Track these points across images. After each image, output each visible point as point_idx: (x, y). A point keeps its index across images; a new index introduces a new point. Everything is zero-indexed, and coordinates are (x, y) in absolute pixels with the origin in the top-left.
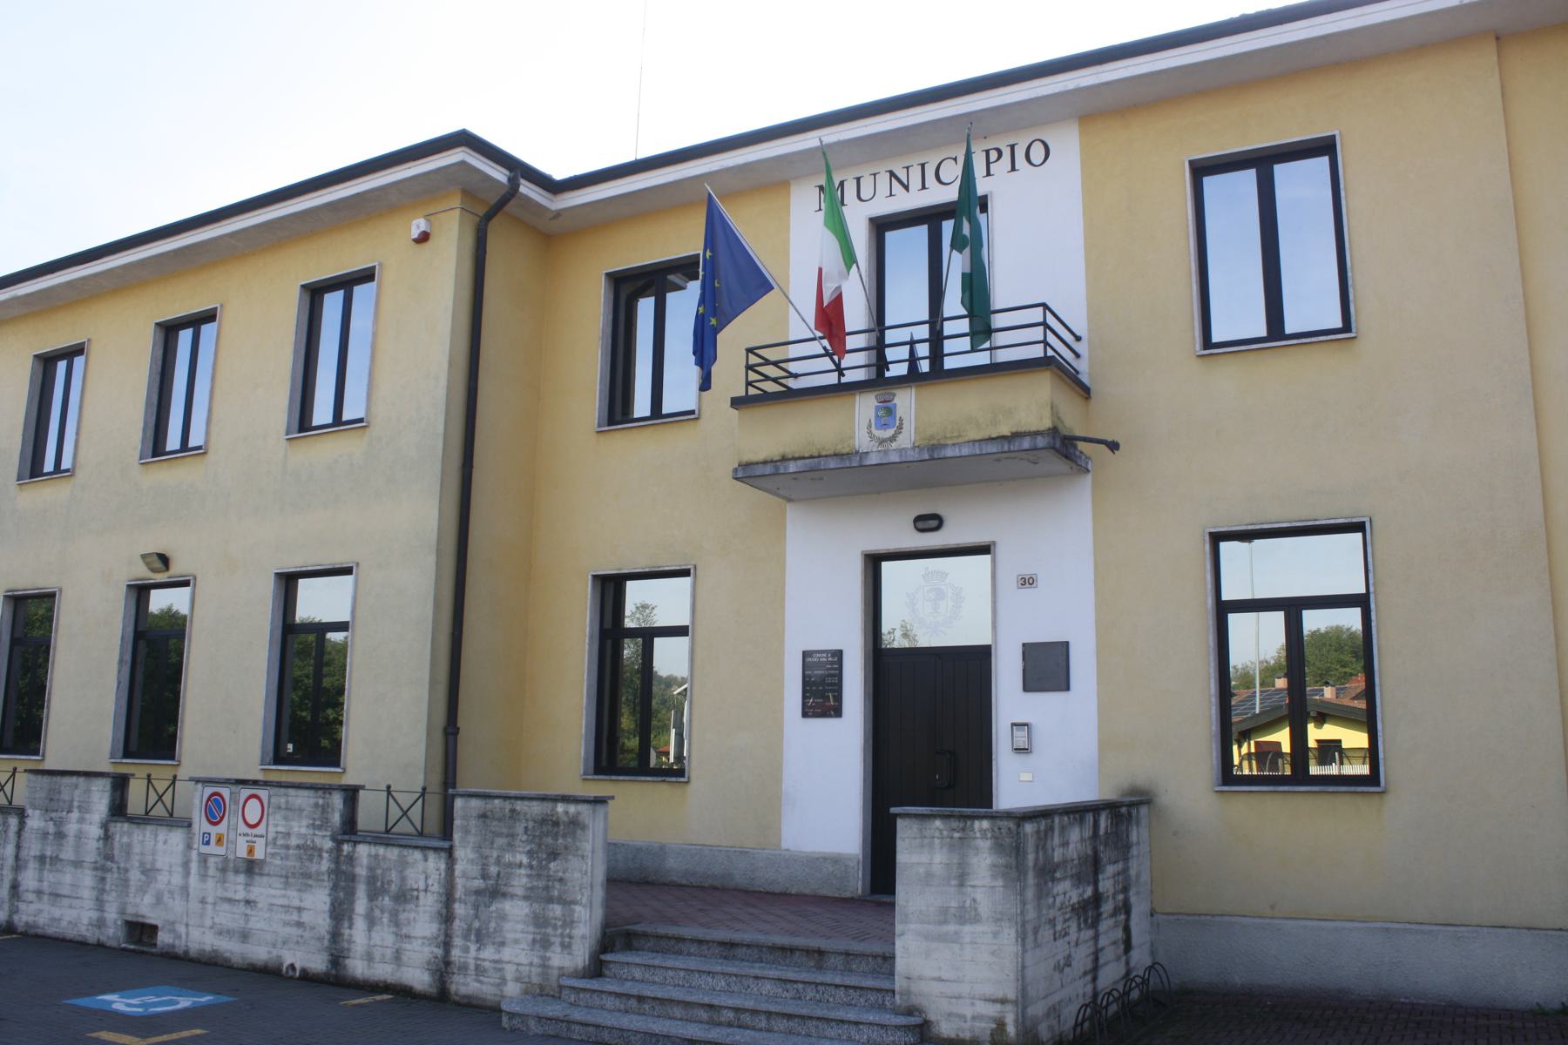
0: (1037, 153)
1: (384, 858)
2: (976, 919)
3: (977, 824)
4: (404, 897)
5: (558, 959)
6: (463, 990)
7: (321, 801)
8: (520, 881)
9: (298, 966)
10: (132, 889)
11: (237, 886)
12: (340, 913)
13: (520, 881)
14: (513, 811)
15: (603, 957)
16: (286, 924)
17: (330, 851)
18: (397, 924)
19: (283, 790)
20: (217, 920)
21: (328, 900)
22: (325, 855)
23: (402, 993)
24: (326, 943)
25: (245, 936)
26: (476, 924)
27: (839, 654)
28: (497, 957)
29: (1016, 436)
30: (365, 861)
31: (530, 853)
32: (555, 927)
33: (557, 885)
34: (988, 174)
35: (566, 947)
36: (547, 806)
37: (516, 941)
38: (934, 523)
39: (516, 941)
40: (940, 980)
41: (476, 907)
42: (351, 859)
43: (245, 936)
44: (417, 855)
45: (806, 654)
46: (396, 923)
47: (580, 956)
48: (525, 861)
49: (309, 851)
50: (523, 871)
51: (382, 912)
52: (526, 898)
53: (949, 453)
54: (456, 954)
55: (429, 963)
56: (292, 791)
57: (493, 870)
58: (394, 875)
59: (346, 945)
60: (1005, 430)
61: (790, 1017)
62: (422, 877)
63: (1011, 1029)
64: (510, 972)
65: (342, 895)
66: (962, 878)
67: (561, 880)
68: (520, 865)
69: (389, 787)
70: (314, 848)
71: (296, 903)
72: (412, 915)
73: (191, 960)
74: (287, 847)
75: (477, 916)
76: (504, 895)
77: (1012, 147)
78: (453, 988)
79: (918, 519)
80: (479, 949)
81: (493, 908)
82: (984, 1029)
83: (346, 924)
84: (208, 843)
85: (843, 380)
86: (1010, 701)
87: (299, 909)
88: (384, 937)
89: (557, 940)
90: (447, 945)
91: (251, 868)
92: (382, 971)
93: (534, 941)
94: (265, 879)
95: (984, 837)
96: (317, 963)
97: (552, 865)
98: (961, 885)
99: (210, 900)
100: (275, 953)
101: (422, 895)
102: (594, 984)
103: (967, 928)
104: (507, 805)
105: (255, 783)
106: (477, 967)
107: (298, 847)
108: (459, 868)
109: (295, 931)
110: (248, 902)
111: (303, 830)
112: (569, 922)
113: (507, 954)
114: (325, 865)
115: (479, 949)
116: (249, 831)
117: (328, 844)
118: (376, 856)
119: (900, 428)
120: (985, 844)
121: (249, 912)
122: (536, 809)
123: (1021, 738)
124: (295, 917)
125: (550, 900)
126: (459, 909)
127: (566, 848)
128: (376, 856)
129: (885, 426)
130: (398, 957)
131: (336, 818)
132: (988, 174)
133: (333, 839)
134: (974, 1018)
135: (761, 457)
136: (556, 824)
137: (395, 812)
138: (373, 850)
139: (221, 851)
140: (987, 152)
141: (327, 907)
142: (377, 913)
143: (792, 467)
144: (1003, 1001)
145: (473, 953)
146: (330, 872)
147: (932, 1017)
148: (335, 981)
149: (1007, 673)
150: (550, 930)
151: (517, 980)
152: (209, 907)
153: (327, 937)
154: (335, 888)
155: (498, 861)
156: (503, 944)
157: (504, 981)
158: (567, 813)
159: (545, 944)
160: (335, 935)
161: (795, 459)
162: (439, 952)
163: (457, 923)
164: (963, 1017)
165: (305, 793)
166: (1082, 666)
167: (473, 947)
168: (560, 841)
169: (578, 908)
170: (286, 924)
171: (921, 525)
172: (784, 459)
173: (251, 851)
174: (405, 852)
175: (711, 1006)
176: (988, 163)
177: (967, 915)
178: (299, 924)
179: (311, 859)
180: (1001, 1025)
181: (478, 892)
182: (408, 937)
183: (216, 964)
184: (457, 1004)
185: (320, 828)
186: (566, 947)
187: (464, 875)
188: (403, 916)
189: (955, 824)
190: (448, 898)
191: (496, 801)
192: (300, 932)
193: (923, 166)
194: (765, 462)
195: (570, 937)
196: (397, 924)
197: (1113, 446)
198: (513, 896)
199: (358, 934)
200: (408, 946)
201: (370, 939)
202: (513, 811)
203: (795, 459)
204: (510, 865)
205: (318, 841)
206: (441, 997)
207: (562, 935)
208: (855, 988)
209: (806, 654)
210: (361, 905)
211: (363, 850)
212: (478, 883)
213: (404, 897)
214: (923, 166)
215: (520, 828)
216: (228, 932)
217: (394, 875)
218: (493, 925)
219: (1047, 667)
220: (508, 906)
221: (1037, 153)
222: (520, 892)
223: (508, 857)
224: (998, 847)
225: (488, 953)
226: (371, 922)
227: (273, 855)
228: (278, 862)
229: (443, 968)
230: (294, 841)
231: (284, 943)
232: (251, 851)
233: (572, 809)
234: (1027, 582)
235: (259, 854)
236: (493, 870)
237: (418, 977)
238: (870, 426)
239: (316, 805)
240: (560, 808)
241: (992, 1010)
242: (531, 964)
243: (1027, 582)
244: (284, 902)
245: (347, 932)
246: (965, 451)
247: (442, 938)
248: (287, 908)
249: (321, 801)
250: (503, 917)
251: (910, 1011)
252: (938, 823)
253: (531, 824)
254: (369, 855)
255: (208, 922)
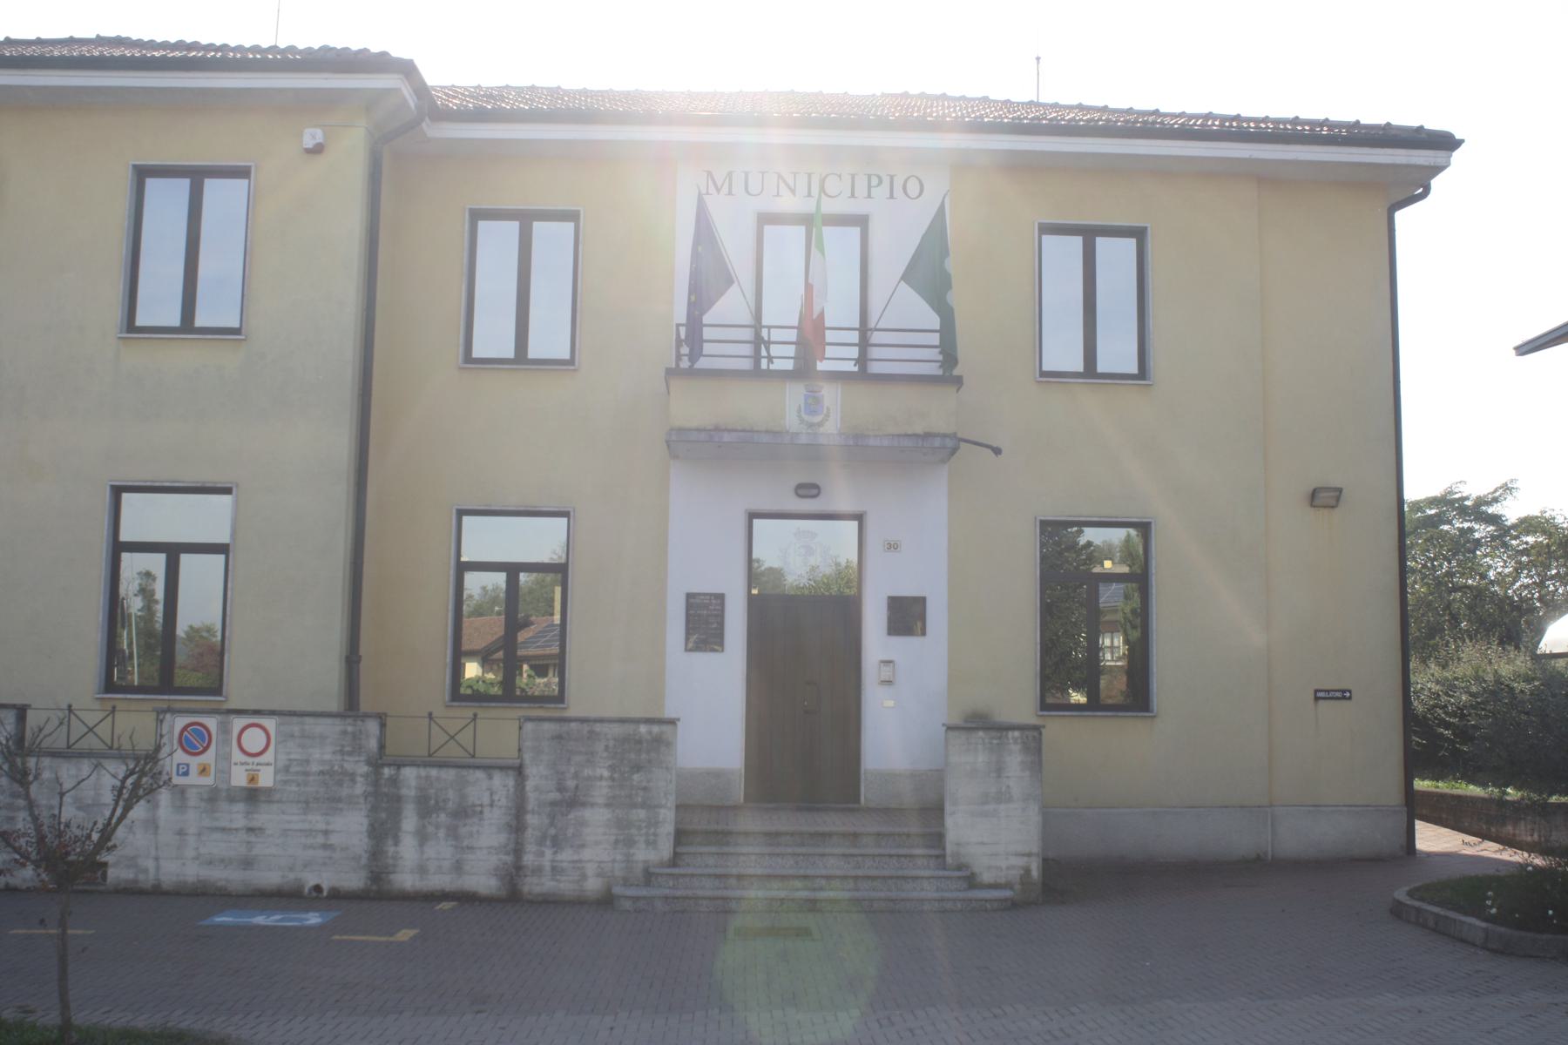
0: (913, 188)
1: (438, 779)
2: (1010, 800)
3: (1010, 734)
4: (464, 812)
5: (642, 854)
6: (537, 889)
7: (350, 729)
8: (601, 792)
9: (325, 886)
10: (317, 820)
11: (236, 816)
12: (382, 832)
13: (601, 792)
14: (591, 732)
15: (679, 850)
16: (306, 847)
17: (366, 776)
18: (456, 837)
19: (295, 719)
20: (203, 850)
21: (365, 822)
22: (359, 779)
23: (466, 898)
24: (364, 861)
25: (247, 863)
26: (552, 831)
27: (720, 598)
28: (576, 858)
29: (928, 436)
30: (413, 783)
31: (612, 768)
32: (639, 828)
33: (641, 793)
34: (869, 196)
35: (651, 843)
36: (630, 728)
37: (597, 843)
38: (814, 492)
39: (597, 843)
40: (983, 843)
41: (552, 817)
42: (394, 781)
43: (247, 863)
44: (480, 774)
45: (689, 596)
46: (453, 833)
47: (665, 849)
48: (606, 774)
49: (336, 776)
50: (604, 783)
51: (437, 827)
52: (607, 805)
53: (872, 442)
54: (529, 859)
55: (496, 869)
56: (308, 720)
57: (571, 784)
58: (451, 794)
59: (391, 861)
60: (919, 429)
61: (869, 878)
62: (487, 794)
63: (1035, 873)
64: (591, 869)
65: (384, 815)
66: (999, 771)
67: (645, 789)
68: (601, 778)
69: (430, 714)
70: (344, 773)
71: (322, 826)
72: (475, 829)
73: (166, 893)
74: (306, 774)
75: (552, 824)
76: (584, 805)
77: (892, 177)
78: (526, 889)
79: (800, 487)
80: (555, 853)
81: (571, 816)
82: (1015, 875)
83: (390, 842)
84: (186, 774)
85: (772, 367)
86: (876, 641)
87: (326, 833)
88: (441, 850)
89: (642, 839)
90: (518, 851)
91: (252, 795)
92: (439, 881)
93: (617, 842)
94: (275, 807)
95: (1015, 742)
96: (354, 880)
97: (636, 777)
98: (999, 776)
99: (192, 830)
100: (292, 876)
101: (487, 810)
102: (676, 871)
103: (1002, 807)
104: (586, 728)
105: (257, 712)
106: (554, 869)
107: (322, 773)
108: (530, 785)
109: (320, 853)
110: (250, 830)
111: (327, 757)
112: (654, 823)
113: (587, 854)
114: (360, 788)
115: (555, 853)
116: (250, 760)
117: (363, 769)
118: (427, 777)
119: (828, 415)
120: (1016, 748)
121: (253, 839)
122: (617, 729)
123: (886, 673)
124: (320, 839)
125: (634, 806)
126: (531, 820)
127: (650, 761)
128: (427, 777)
129: (813, 412)
130: (458, 867)
131: (373, 744)
132: (869, 196)
133: (369, 763)
134: (1008, 868)
135: (694, 424)
136: (640, 742)
137: (439, 738)
138: (423, 772)
139: (208, 781)
140: (869, 177)
141: (364, 828)
142: (430, 829)
143: (727, 437)
144: (1029, 855)
145: (548, 853)
146: (366, 796)
147: (976, 870)
148: (377, 895)
149: (874, 618)
150: (634, 831)
151: (598, 875)
152: (191, 840)
153: (365, 856)
154: (374, 809)
155: (576, 776)
156: (583, 846)
157: (584, 877)
158: (650, 733)
159: (630, 842)
160: (376, 854)
161: (729, 431)
162: (509, 859)
163: (529, 832)
164: (999, 868)
165: (329, 721)
166: (937, 615)
167: (548, 853)
168: (644, 756)
169: (663, 811)
170: (306, 847)
171: (801, 492)
172: (717, 429)
173: (252, 779)
174: (464, 772)
175: (805, 877)
176: (870, 187)
177: (1003, 797)
178: (325, 847)
179: (340, 784)
180: (1027, 871)
181: (553, 804)
182: (470, 848)
183: (204, 894)
184: (531, 902)
185: (350, 754)
186: (651, 843)
187: (536, 788)
188: (463, 831)
189: (994, 734)
190: (519, 810)
191: (573, 725)
192: (328, 853)
193: (809, 175)
194: (698, 430)
195: (655, 835)
196: (456, 837)
197: (997, 451)
198: (592, 805)
199: (407, 850)
200: (470, 856)
201: (422, 853)
202: (591, 732)
203: (729, 431)
204: (589, 778)
205: (349, 767)
206: (512, 897)
207: (647, 834)
208: (905, 856)
209: (689, 596)
210: (409, 822)
211: (409, 774)
212: (555, 796)
213: (464, 812)
214: (809, 175)
215: (599, 747)
216: (222, 861)
217: (451, 794)
218: (570, 831)
219: (907, 616)
220: (588, 813)
221: (913, 188)
222: (601, 801)
223: (587, 772)
224: (1026, 749)
225: (566, 855)
226: (422, 837)
227: (285, 782)
228: (294, 788)
229: (513, 873)
230: (314, 768)
231: (305, 866)
232: (252, 779)
233: (656, 729)
234: (892, 547)
235: (266, 779)
236: (571, 784)
237: (482, 879)
238: (799, 411)
239: (345, 733)
240: (643, 729)
241: (1021, 861)
242: (614, 861)
243: (892, 547)
244: (306, 826)
245: (391, 850)
246: (886, 443)
247: (512, 846)
248: (309, 833)
249: (350, 729)
250: (582, 823)
251: (959, 868)
252: (981, 734)
253: (611, 743)
254: (419, 777)
255: (190, 853)
